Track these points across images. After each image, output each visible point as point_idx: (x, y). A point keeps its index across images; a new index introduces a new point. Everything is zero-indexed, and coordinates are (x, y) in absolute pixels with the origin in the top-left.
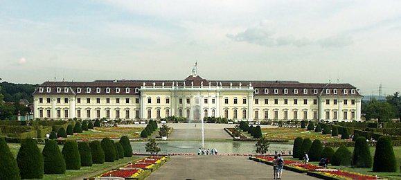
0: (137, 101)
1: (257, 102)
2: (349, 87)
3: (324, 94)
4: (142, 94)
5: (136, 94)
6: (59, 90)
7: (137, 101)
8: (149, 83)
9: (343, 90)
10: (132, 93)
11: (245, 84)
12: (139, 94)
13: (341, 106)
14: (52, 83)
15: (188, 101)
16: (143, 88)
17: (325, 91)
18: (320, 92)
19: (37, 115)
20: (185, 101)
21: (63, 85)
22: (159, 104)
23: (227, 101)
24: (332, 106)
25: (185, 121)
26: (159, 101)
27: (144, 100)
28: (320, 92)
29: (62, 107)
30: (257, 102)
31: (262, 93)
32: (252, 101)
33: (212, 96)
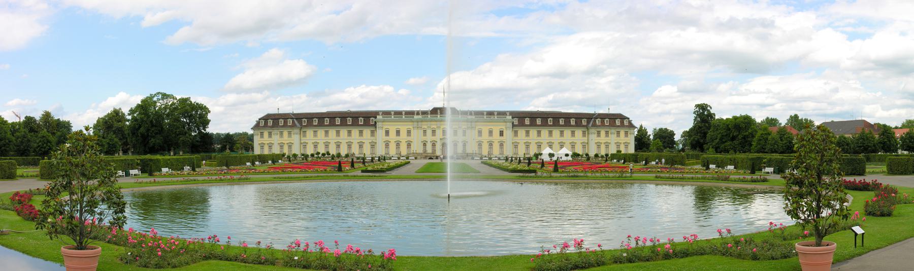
0: (373, 133)
1: (516, 133)
2: (622, 118)
3: (594, 125)
4: (379, 125)
5: (372, 125)
6: (281, 122)
7: (373, 133)
8: (387, 113)
9: (616, 121)
10: (367, 124)
11: (502, 114)
12: (375, 125)
13: (613, 138)
14: (274, 115)
15: (434, 132)
16: (379, 117)
17: (595, 121)
18: (588, 123)
19: (257, 151)
20: (429, 132)
21: (285, 117)
22: (398, 138)
23: (480, 133)
24: (603, 138)
25: (437, 157)
26: (398, 133)
27: (380, 133)
28: (588, 123)
29: (286, 142)
30: (516, 133)
31: (522, 124)
32: (509, 133)
33: (463, 127)
